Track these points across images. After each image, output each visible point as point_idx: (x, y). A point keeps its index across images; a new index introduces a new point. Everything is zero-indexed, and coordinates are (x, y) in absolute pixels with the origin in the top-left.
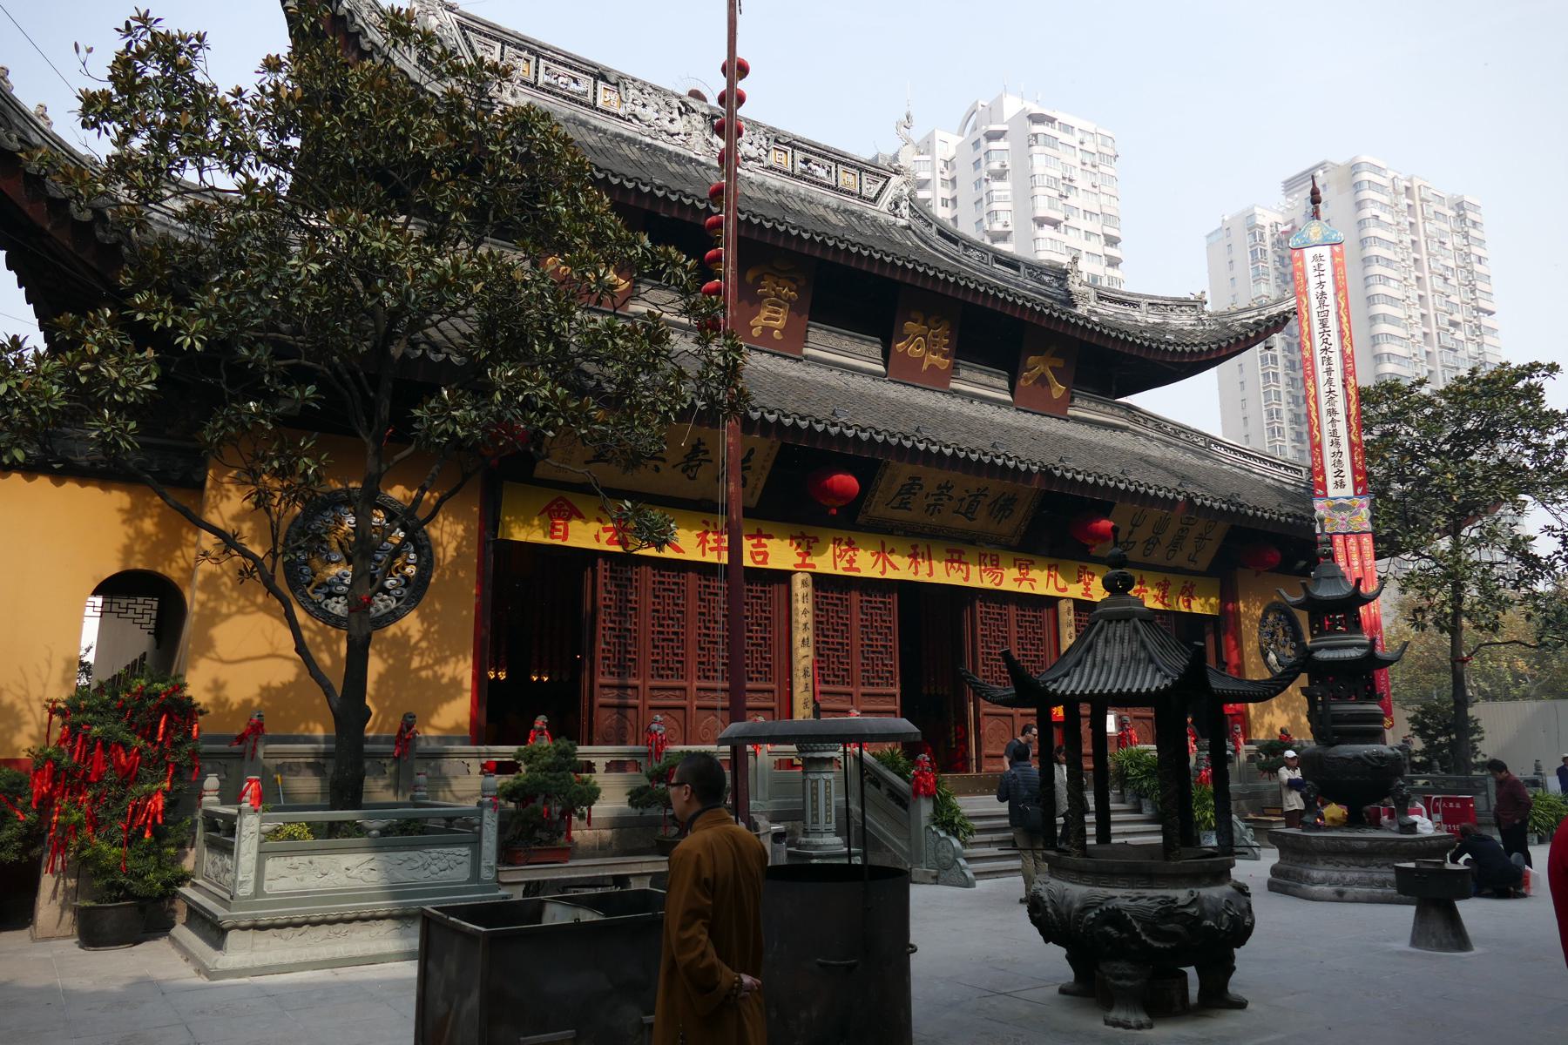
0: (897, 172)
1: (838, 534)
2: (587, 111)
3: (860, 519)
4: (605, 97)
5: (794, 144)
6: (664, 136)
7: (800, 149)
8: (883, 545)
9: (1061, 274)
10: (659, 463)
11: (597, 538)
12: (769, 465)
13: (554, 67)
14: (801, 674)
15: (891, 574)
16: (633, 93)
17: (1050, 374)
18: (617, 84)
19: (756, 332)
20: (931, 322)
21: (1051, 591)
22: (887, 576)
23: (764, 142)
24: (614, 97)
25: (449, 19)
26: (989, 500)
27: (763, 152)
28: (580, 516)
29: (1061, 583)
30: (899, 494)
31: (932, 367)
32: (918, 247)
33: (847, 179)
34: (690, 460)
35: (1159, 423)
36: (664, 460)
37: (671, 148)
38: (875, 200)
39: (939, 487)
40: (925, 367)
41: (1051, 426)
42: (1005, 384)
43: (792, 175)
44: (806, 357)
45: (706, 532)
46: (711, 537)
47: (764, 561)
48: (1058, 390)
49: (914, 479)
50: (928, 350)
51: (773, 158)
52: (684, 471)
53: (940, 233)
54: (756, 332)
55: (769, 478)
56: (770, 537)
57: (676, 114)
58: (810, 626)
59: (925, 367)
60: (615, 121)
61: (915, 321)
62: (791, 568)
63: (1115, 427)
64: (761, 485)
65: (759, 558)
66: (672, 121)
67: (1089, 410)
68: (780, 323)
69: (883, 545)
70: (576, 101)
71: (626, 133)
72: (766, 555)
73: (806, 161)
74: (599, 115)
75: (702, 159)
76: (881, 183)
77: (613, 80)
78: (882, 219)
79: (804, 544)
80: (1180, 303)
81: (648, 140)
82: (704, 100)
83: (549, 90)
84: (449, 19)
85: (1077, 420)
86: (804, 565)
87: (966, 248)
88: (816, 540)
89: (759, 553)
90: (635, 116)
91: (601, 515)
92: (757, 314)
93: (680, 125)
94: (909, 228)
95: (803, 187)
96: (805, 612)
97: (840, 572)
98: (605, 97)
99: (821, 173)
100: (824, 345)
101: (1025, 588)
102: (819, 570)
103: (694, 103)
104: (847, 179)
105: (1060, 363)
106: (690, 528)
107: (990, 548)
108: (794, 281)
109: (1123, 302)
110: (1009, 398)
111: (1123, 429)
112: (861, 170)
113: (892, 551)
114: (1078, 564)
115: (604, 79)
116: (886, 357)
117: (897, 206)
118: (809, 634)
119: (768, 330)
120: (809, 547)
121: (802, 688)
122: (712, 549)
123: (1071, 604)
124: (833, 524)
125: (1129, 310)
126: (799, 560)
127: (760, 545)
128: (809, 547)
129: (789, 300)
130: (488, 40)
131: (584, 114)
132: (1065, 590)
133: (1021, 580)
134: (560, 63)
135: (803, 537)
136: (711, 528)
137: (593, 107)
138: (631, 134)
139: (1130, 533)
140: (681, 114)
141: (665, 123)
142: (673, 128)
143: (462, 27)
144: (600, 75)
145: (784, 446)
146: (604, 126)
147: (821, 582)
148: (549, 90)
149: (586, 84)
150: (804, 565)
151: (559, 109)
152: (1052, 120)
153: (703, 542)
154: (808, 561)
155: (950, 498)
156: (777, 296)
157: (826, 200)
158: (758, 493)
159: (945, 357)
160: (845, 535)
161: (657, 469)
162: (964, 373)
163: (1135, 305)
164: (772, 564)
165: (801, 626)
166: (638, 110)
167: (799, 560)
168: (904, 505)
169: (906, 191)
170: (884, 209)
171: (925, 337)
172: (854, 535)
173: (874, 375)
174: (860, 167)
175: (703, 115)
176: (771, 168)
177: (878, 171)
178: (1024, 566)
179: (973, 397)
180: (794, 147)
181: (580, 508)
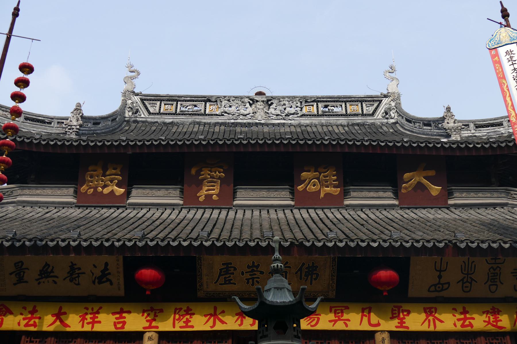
0: (385, 96)
1: (179, 305)
2: (200, 117)
3: (200, 294)
5: (317, 100)
6: (241, 117)
7: (321, 102)
8: (215, 309)
10: (55, 279)
11: (19, 324)
12: (121, 269)
13: (184, 103)
15: (219, 327)
16: (224, 102)
18: (216, 101)
19: (201, 199)
21: (365, 327)
22: (216, 328)
23: (299, 105)
25: (137, 99)
27: (299, 109)
28: (11, 313)
29: (374, 319)
31: (327, 195)
33: (356, 108)
36: (57, 277)
37: (245, 121)
38: (373, 114)
39: (249, 267)
40: (322, 195)
41: (441, 215)
42: (390, 194)
43: (318, 115)
45: (86, 314)
46: (88, 317)
47: (123, 327)
48: (435, 190)
49: (227, 265)
50: (322, 185)
51: (305, 110)
52: (71, 281)
53: (407, 120)
54: (201, 199)
55: (125, 277)
56: (129, 312)
57: (248, 105)
59: (322, 195)
60: (215, 118)
62: (141, 329)
63: (494, 206)
65: (119, 326)
67: (466, 198)
68: (217, 191)
69: (215, 309)
70: (196, 115)
71: (220, 121)
72: (124, 323)
74: (207, 117)
75: (263, 122)
76: (376, 105)
77: (213, 100)
78: (378, 122)
79: (152, 315)
81: (233, 121)
82: (264, 94)
83: (183, 113)
84: (137, 99)
85: (456, 206)
86: (150, 327)
88: (161, 311)
89: (119, 323)
90: (226, 112)
91: (23, 311)
92: (201, 189)
93: (250, 110)
94: (396, 123)
97: (177, 329)
98: (210, 108)
100: (245, 197)
101: (340, 326)
102: (161, 329)
104: (351, 108)
105: (431, 173)
106: (76, 312)
107: (91, 302)
108: (221, 167)
109: (492, 125)
112: (361, 102)
113: (223, 312)
114: (391, 306)
115: (209, 100)
119: (209, 197)
120: (156, 316)
122: (88, 323)
123: (386, 335)
124: (388, 300)
125: (497, 129)
126: (147, 324)
127: (121, 317)
128: (156, 316)
129: (220, 178)
130: (154, 102)
131: (198, 119)
132: (379, 325)
133: (335, 321)
134: (188, 101)
135: (152, 310)
136: (90, 311)
137: (205, 114)
138: (223, 121)
139: (440, 277)
140: (251, 105)
141: (242, 111)
142: (246, 113)
143: (142, 100)
144: (207, 100)
145: (125, 258)
146: (209, 121)
147: (163, 335)
148: (183, 113)
149: (201, 106)
150: (150, 327)
151: (186, 120)
153: (83, 319)
154: (154, 324)
155: (262, 273)
157: (339, 122)
158: (122, 287)
159: (335, 186)
160: (184, 306)
161: (55, 283)
162: (353, 194)
163: (500, 124)
164: (128, 328)
166: (226, 109)
167: (147, 324)
168: (228, 282)
169: (393, 104)
170: (380, 117)
171: (318, 179)
172: (191, 305)
174: (361, 100)
175: (263, 101)
177: (375, 100)
178: (339, 312)
179: (361, 207)
180: (319, 101)
181: (12, 309)
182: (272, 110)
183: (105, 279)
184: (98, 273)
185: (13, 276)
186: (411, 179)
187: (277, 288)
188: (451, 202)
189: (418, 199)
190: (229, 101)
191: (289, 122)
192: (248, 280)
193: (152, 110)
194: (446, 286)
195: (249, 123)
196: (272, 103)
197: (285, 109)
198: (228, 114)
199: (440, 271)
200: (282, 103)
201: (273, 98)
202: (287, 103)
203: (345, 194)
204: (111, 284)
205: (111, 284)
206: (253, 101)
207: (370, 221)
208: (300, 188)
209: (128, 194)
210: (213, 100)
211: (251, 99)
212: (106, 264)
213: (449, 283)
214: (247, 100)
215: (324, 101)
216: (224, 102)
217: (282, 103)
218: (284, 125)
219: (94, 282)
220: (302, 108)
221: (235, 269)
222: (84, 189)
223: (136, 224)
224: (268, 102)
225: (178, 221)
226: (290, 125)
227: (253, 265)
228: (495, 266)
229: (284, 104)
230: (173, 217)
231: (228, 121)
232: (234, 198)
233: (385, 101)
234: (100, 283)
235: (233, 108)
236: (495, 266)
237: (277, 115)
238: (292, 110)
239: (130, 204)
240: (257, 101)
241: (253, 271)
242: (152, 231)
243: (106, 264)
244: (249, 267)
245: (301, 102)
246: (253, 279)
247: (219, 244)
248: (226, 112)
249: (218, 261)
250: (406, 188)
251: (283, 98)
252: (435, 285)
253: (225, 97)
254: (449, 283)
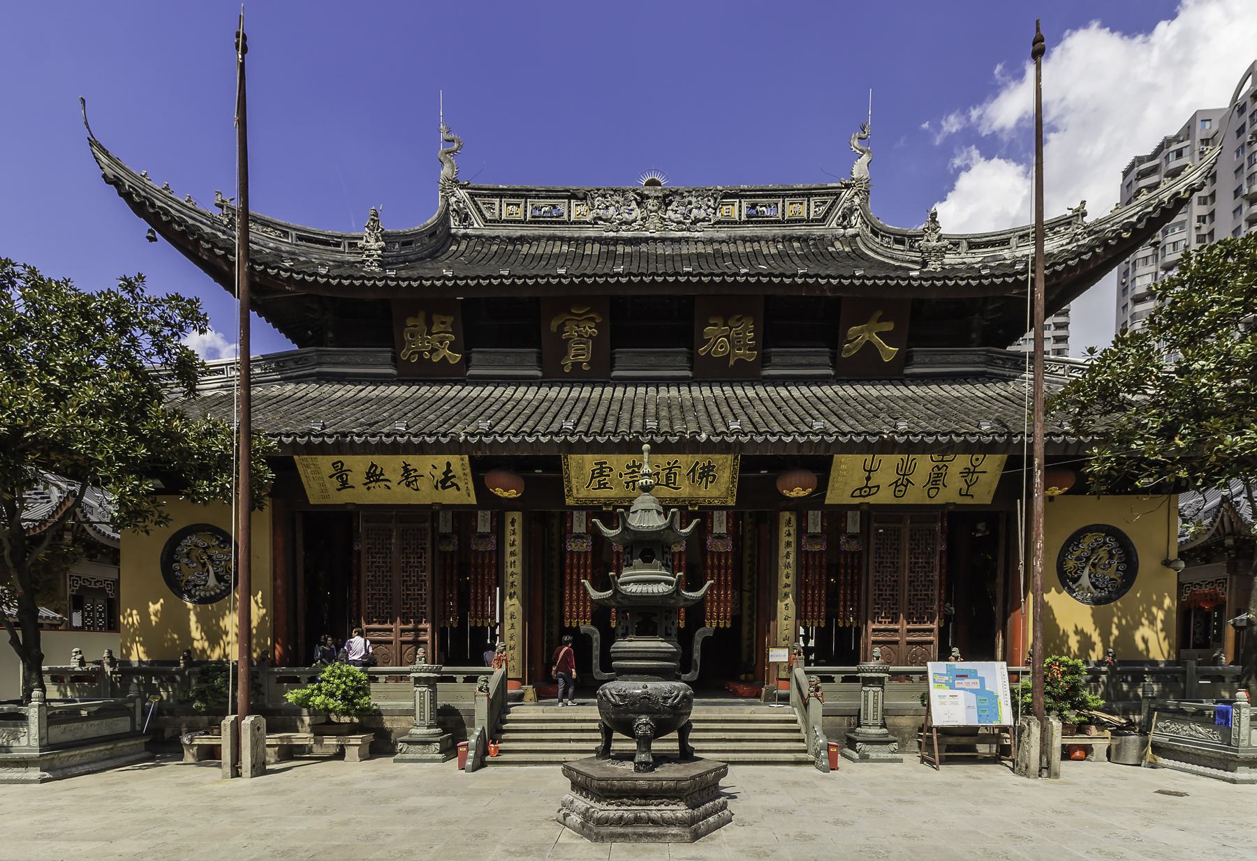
12: (468, 471)
24: (583, 209)
25: (462, 194)
26: (685, 472)
30: (593, 477)
31: (740, 362)
34: (407, 478)
40: (732, 363)
42: (827, 360)
48: (889, 352)
52: (408, 486)
57: (634, 205)
59: (732, 363)
64: (471, 486)
75: (657, 235)
76: (830, 200)
77: (581, 195)
90: (600, 219)
119: (577, 365)
129: (591, 337)
139: (868, 479)
140: (639, 204)
142: (630, 218)
145: (471, 458)
158: (472, 493)
168: (603, 486)
175: (657, 198)
176: (718, 222)
183: (449, 483)
184: (439, 475)
185: (334, 479)
187: (645, 510)
188: (908, 371)
189: (866, 368)
190: (604, 196)
191: (697, 234)
192: (628, 483)
193: (488, 216)
194: (874, 490)
195: (636, 239)
196: (671, 202)
197: (690, 211)
198: (605, 221)
199: (870, 471)
200: (686, 200)
202: (694, 200)
203: (764, 360)
204: (458, 489)
205: (458, 489)
207: (792, 401)
208: (702, 350)
209: (466, 362)
210: (581, 195)
211: (638, 194)
212: (449, 464)
213: (878, 487)
214: (631, 195)
218: (687, 240)
219: (436, 487)
220: (715, 209)
221: (611, 470)
222: (405, 355)
223: (481, 409)
225: (535, 403)
226: (696, 241)
227: (634, 466)
228: (941, 464)
229: (690, 203)
230: (530, 396)
231: (605, 234)
232: (612, 368)
233: (846, 194)
234: (444, 487)
235: (612, 209)
236: (941, 464)
237: (679, 223)
238: (702, 214)
239: (471, 377)
240: (648, 198)
241: (634, 472)
242: (502, 419)
243: (449, 464)
244: (628, 467)
245: (715, 199)
246: (634, 482)
247: (587, 440)
248: (600, 219)
249: (589, 461)
250: (849, 350)
252: (861, 489)
254: (878, 487)
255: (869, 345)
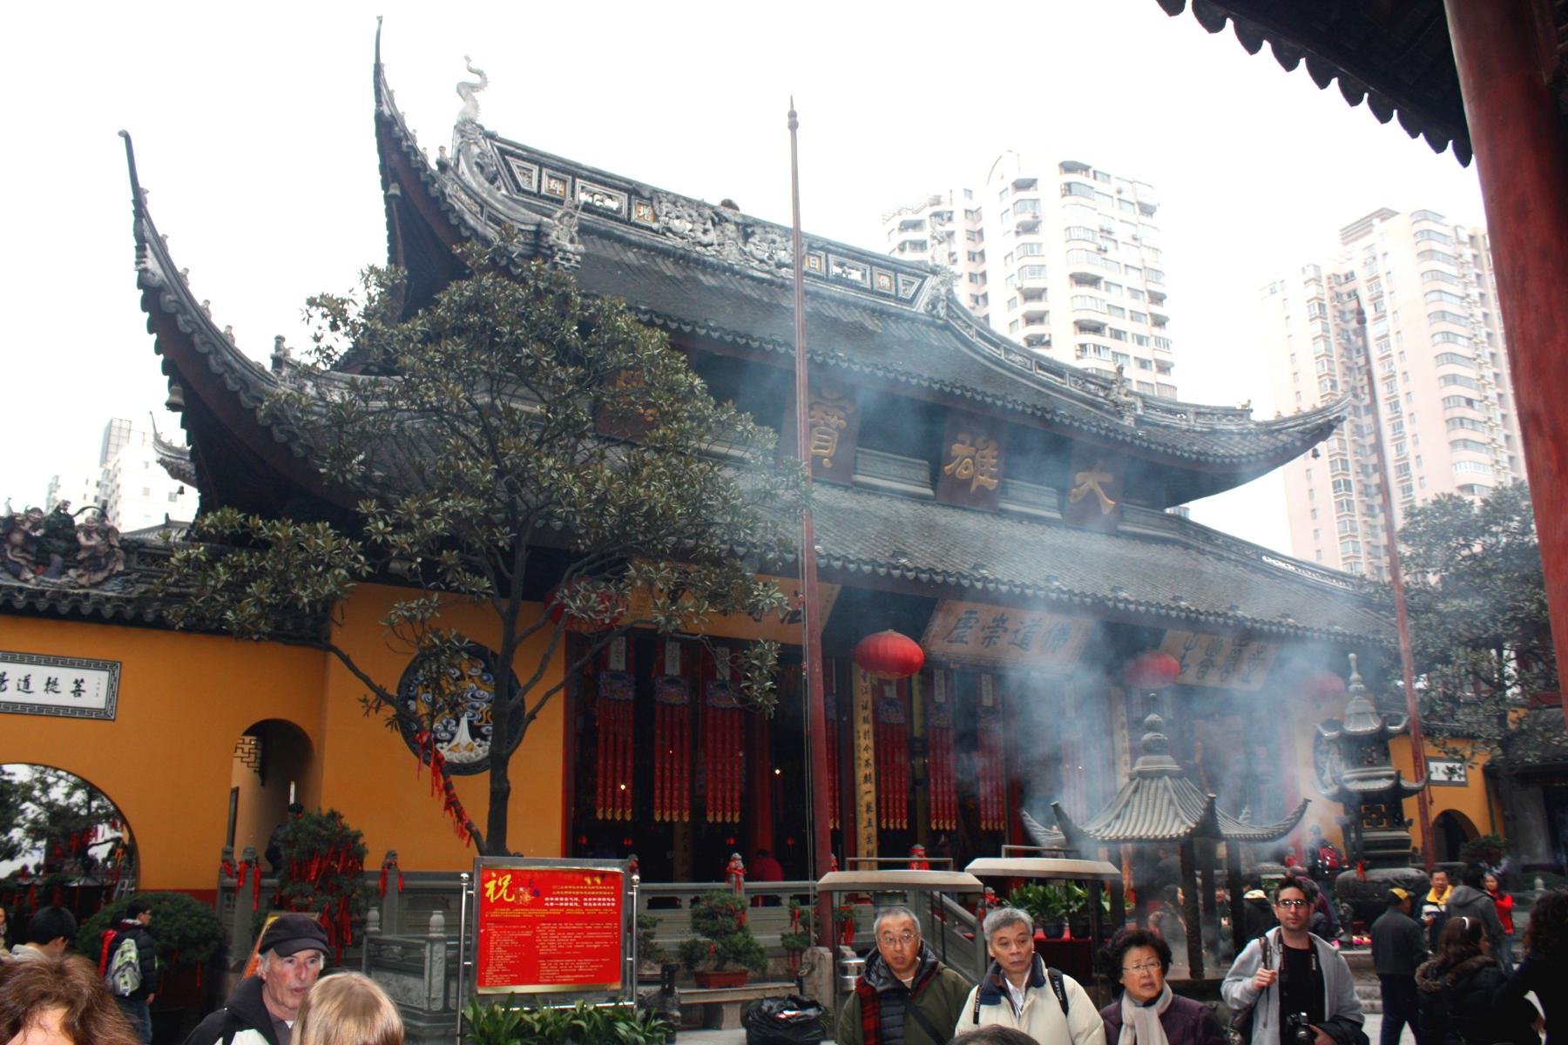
0: (934, 272)
4: (642, 213)
9: (1106, 385)
13: (590, 186)
14: (864, 809)
16: (666, 207)
17: (1099, 490)
18: (651, 199)
20: (979, 441)
32: (957, 350)
35: (1206, 534)
38: (911, 302)
40: (973, 488)
42: (1054, 501)
44: (856, 484)
57: (709, 225)
58: (872, 762)
61: (963, 443)
66: (705, 232)
73: (841, 265)
74: (633, 230)
76: (917, 284)
77: (647, 194)
80: (1229, 413)
87: (1007, 351)
90: (669, 230)
95: (837, 290)
96: (866, 749)
99: (855, 275)
103: (727, 213)
105: (1108, 478)
110: (1057, 516)
111: (1174, 542)
112: (896, 271)
116: (934, 479)
117: (934, 307)
118: (870, 770)
121: (865, 823)
137: (628, 222)
140: (714, 224)
142: (706, 239)
143: (503, 152)
144: (634, 191)
152: (1086, 168)
156: (827, 425)
165: (863, 763)
169: (943, 290)
170: (922, 310)
171: (973, 458)
173: (922, 499)
175: (737, 224)
182: (749, 248)
186: (1086, 481)
190: (674, 204)
196: (753, 233)
198: (675, 234)
200: (771, 236)
201: (757, 223)
206: (719, 220)
214: (708, 212)
215: (841, 255)
216: (666, 207)
217: (771, 236)
224: (747, 228)
229: (774, 242)
251: (772, 226)
253: (668, 193)
255: (1091, 491)
